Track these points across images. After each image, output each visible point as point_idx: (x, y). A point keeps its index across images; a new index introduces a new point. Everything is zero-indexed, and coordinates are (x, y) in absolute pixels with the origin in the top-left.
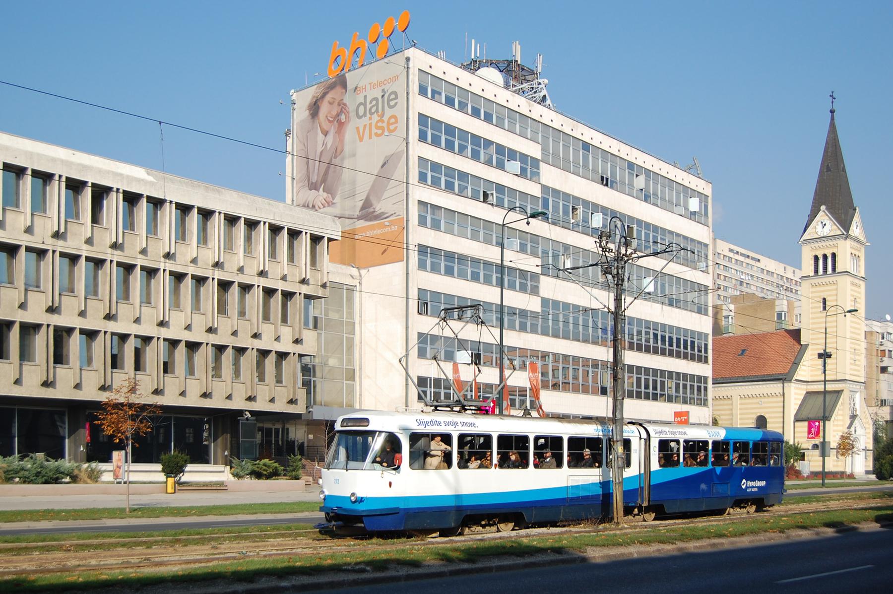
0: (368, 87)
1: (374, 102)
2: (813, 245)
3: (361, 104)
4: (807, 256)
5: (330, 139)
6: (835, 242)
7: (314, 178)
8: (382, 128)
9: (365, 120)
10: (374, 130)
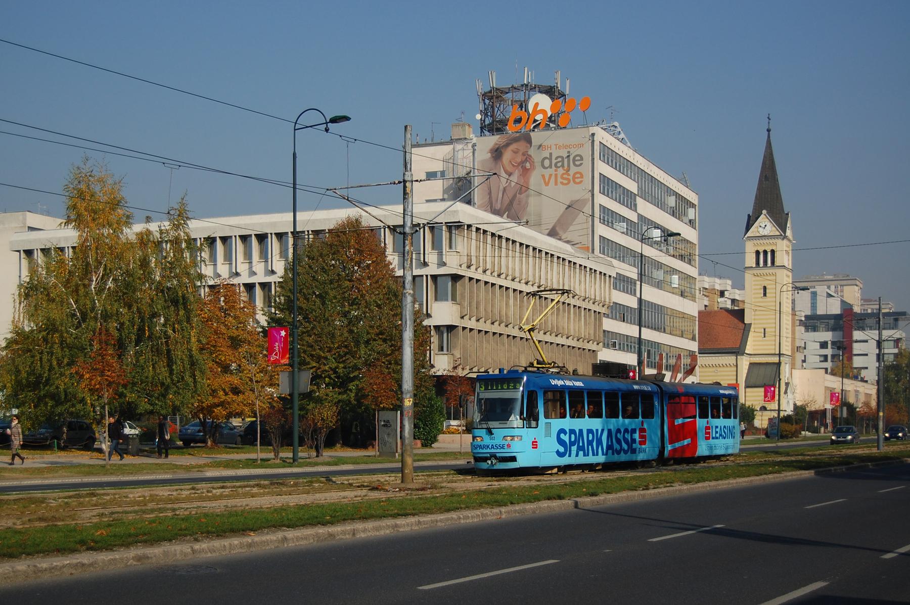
0: (553, 147)
1: (560, 159)
2: (755, 242)
3: (546, 158)
4: (750, 248)
5: (514, 178)
6: (774, 241)
7: (498, 206)
8: (568, 179)
9: (552, 171)
10: (559, 180)
